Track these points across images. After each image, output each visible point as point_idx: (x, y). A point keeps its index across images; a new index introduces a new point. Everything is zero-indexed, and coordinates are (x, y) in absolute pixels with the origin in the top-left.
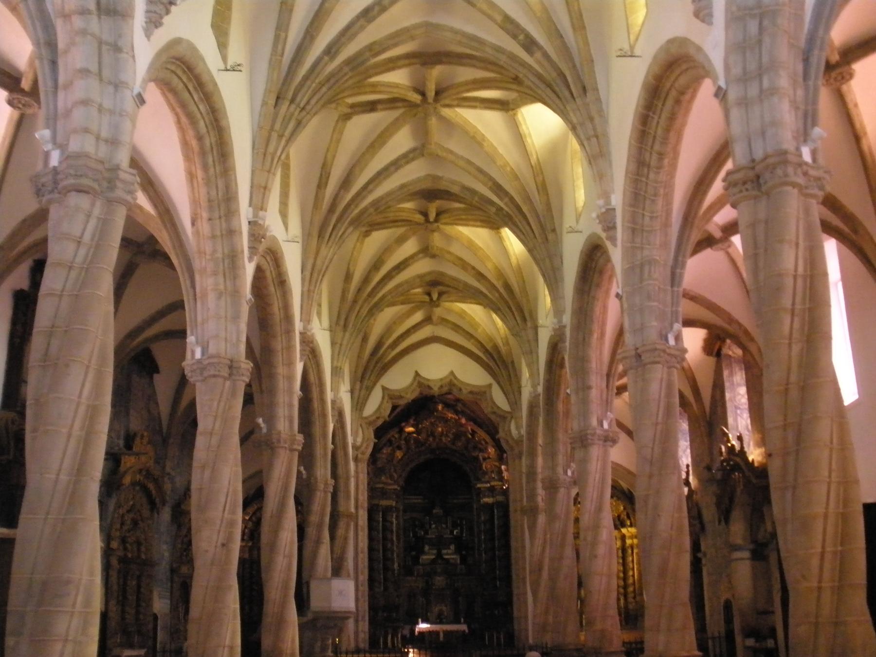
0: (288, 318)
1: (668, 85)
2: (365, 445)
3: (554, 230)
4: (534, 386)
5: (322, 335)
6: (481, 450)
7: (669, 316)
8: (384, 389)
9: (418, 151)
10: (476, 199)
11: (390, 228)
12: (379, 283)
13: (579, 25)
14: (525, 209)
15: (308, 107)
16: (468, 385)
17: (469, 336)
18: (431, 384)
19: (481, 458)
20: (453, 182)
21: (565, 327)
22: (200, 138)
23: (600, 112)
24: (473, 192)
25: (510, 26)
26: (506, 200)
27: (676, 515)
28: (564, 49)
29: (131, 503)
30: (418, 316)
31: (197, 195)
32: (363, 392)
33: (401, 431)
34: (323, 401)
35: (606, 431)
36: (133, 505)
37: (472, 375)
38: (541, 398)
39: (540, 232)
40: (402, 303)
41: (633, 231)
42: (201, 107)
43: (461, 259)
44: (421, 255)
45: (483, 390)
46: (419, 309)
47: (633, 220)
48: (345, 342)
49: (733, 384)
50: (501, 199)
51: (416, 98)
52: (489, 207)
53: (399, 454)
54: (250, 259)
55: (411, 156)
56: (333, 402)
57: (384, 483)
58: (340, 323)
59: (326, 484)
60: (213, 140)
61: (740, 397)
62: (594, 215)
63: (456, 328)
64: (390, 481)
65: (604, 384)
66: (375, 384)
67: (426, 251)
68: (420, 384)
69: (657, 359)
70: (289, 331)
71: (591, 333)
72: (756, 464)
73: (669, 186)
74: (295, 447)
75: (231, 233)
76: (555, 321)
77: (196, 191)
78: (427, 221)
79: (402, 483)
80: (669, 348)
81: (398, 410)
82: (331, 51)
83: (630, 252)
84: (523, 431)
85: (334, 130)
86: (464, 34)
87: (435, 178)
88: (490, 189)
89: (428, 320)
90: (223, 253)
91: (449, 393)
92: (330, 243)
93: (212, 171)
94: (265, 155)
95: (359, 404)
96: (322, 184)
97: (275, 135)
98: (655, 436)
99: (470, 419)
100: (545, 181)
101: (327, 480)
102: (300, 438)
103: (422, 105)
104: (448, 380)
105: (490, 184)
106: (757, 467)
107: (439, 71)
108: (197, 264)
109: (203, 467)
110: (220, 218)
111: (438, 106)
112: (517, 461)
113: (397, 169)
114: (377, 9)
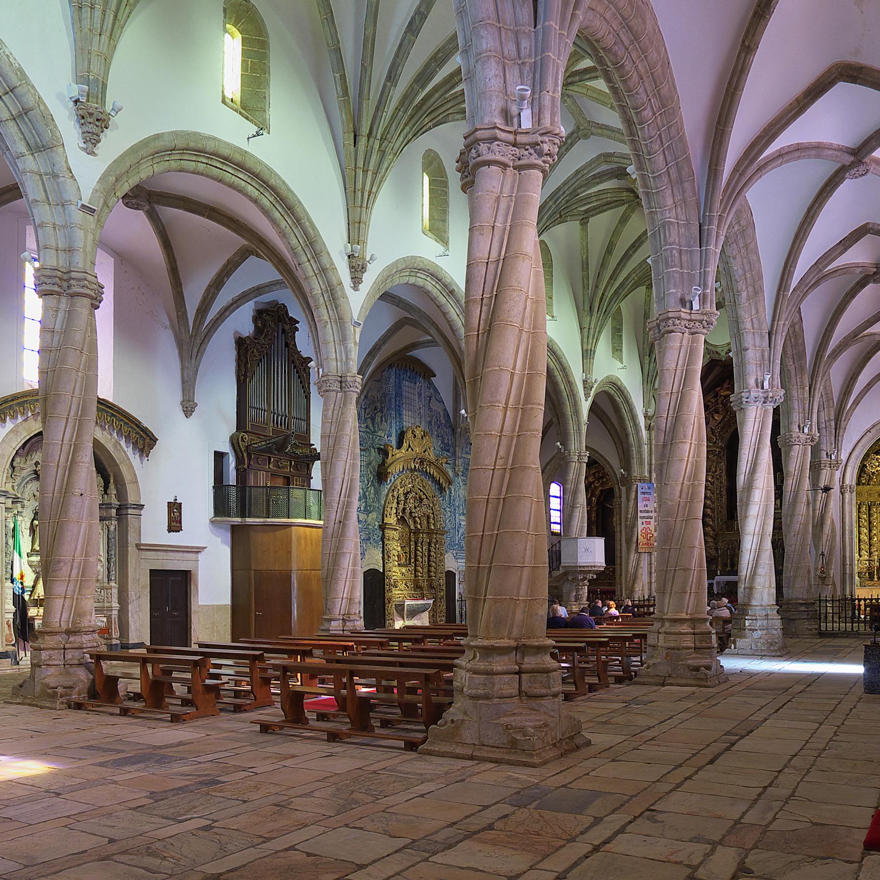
9: (575, 135)
18: (719, 350)
54: (355, 288)
82: (392, 77)
97: (360, 173)
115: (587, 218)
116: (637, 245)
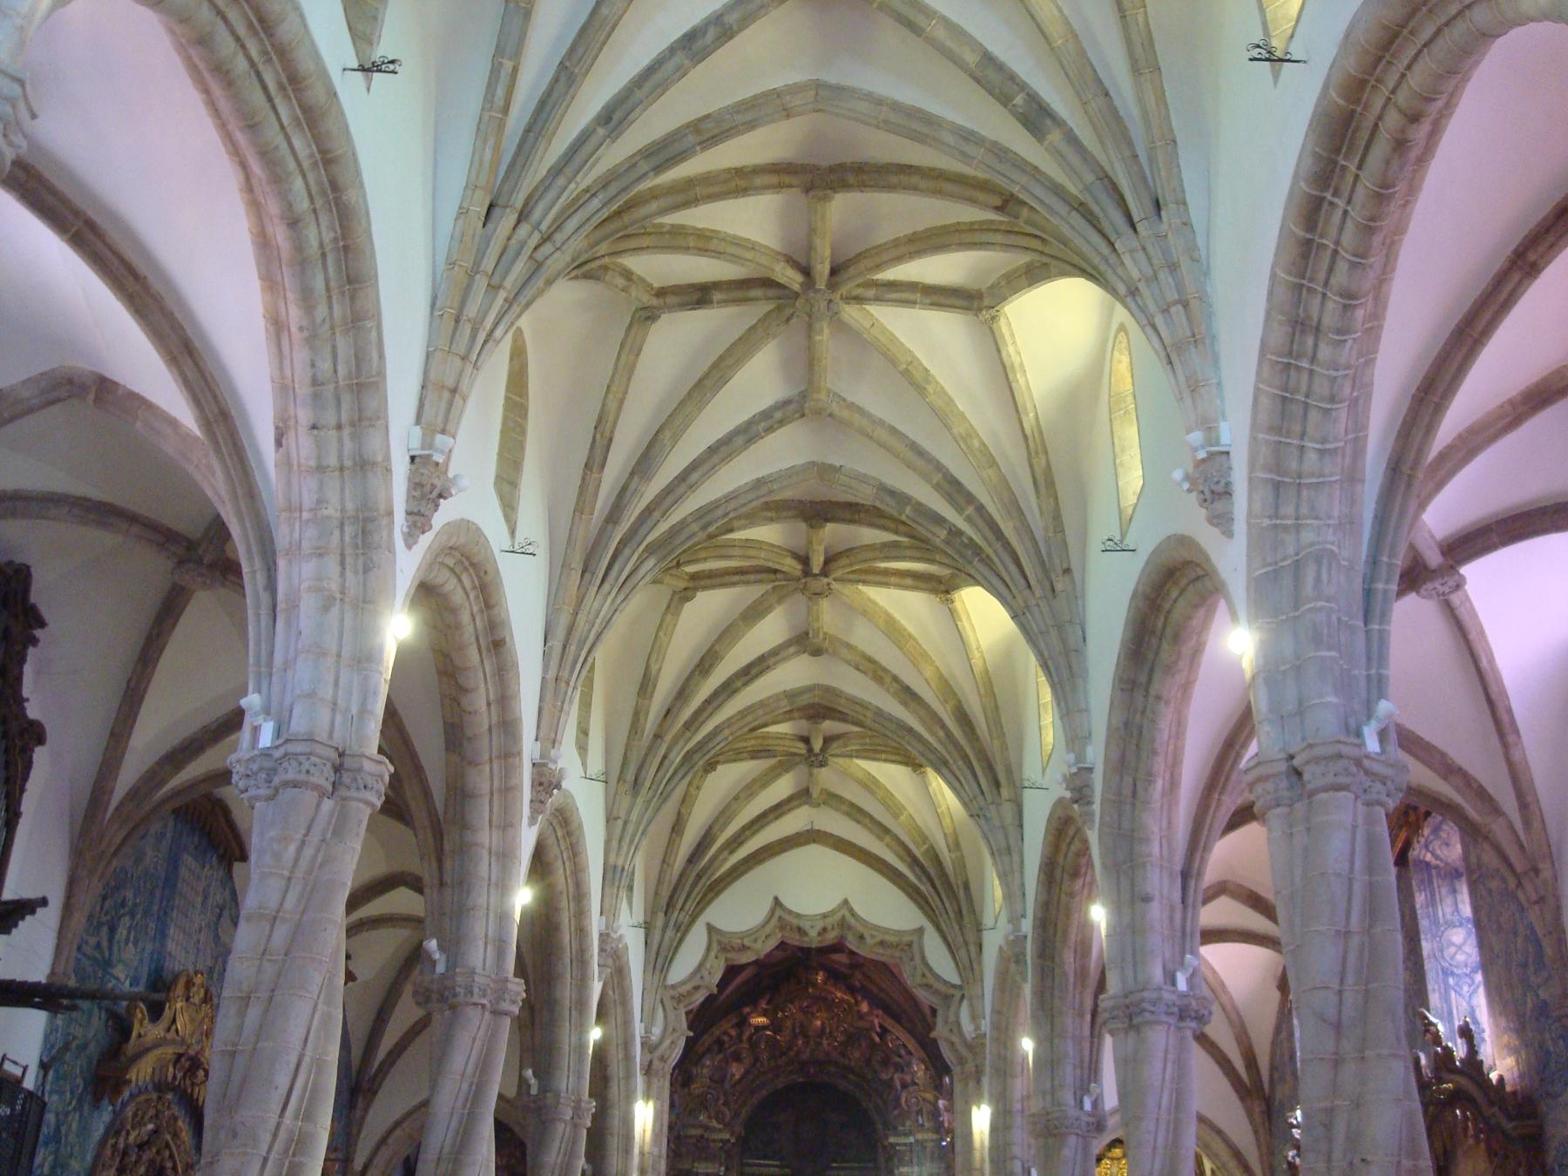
0: (508, 726)
1: (1378, 103)
2: (667, 1042)
3: (1067, 571)
4: (1015, 919)
5: (586, 797)
6: (900, 1068)
7: (1363, 683)
8: (711, 929)
9: (792, 406)
10: (908, 510)
11: (734, 584)
12: (708, 702)
13: (1144, 62)
14: (1008, 529)
15: (559, 238)
16: (877, 928)
17: (882, 830)
18: (806, 925)
19: (898, 1084)
20: (861, 478)
21: (1090, 770)
22: (294, 223)
23: (1191, 249)
24: (902, 498)
25: (994, 79)
26: (970, 510)
27: (1407, 1163)
28: (1112, 121)
29: (151, 1126)
30: (783, 787)
31: (288, 373)
32: (670, 933)
33: (743, 1022)
34: (581, 932)
35: (1183, 995)
36: (155, 1131)
37: (886, 910)
38: (1029, 948)
39: (1039, 583)
40: (755, 754)
41: (1277, 486)
42: (298, 143)
43: (871, 660)
44: (792, 650)
45: (906, 939)
46: (787, 771)
47: (1278, 466)
48: (634, 817)
49: (1436, 923)
50: (960, 510)
51: (792, 278)
52: (936, 529)
53: (736, 1071)
55: (778, 415)
56: (604, 937)
57: (706, 1128)
58: (630, 777)
59: (577, 1108)
60: (328, 236)
61: (1452, 950)
62: (1178, 474)
63: (856, 813)
64: (714, 1123)
65: (1177, 895)
66: (694, 918)
67: (805, 642)
68: (783, 925)
69: (1342, 780)
70: (509, 754)
71: (1150, 778)
72: (1508, 1088)
73: (1363, 387)
74: (505, 1006)
75: (365, 466)
76: (1071, 757)
77: (287, 363)
78: (807, 572)
79: (739, 1129)
80: (1367, 756)
81: (739, 980)
82: (613, 118)
83: (1267, 538)
84: (986, 1025)
85: (622, 346)
86: (896, 107)
87: (825, 471)
88: (937, 487)
89: (802, 796)
90: (343, 510)
91: (838, 947)
92: (606, 587)
93: (321, 311)
94: (457, 321)
95: (659, 960)
96: (595, 461)
97: (481, 283)
98: (1344, 959)
99: (876, 1002)
100: (1052, 465)
101: (579, 1101)
102: (517, 987)
103: (801, 293)
104: (838, 917)
105: (937, 477)
106: (1514, 1093)
107: (844, 218)
108: (283, 536)
109: (246, 1000)
110: (339, 427)
111: (836, 297)
112: (972, 1084)
113: (749, 442)
114: (712, 33)
115: (696, 589)
116: (754, 671)
